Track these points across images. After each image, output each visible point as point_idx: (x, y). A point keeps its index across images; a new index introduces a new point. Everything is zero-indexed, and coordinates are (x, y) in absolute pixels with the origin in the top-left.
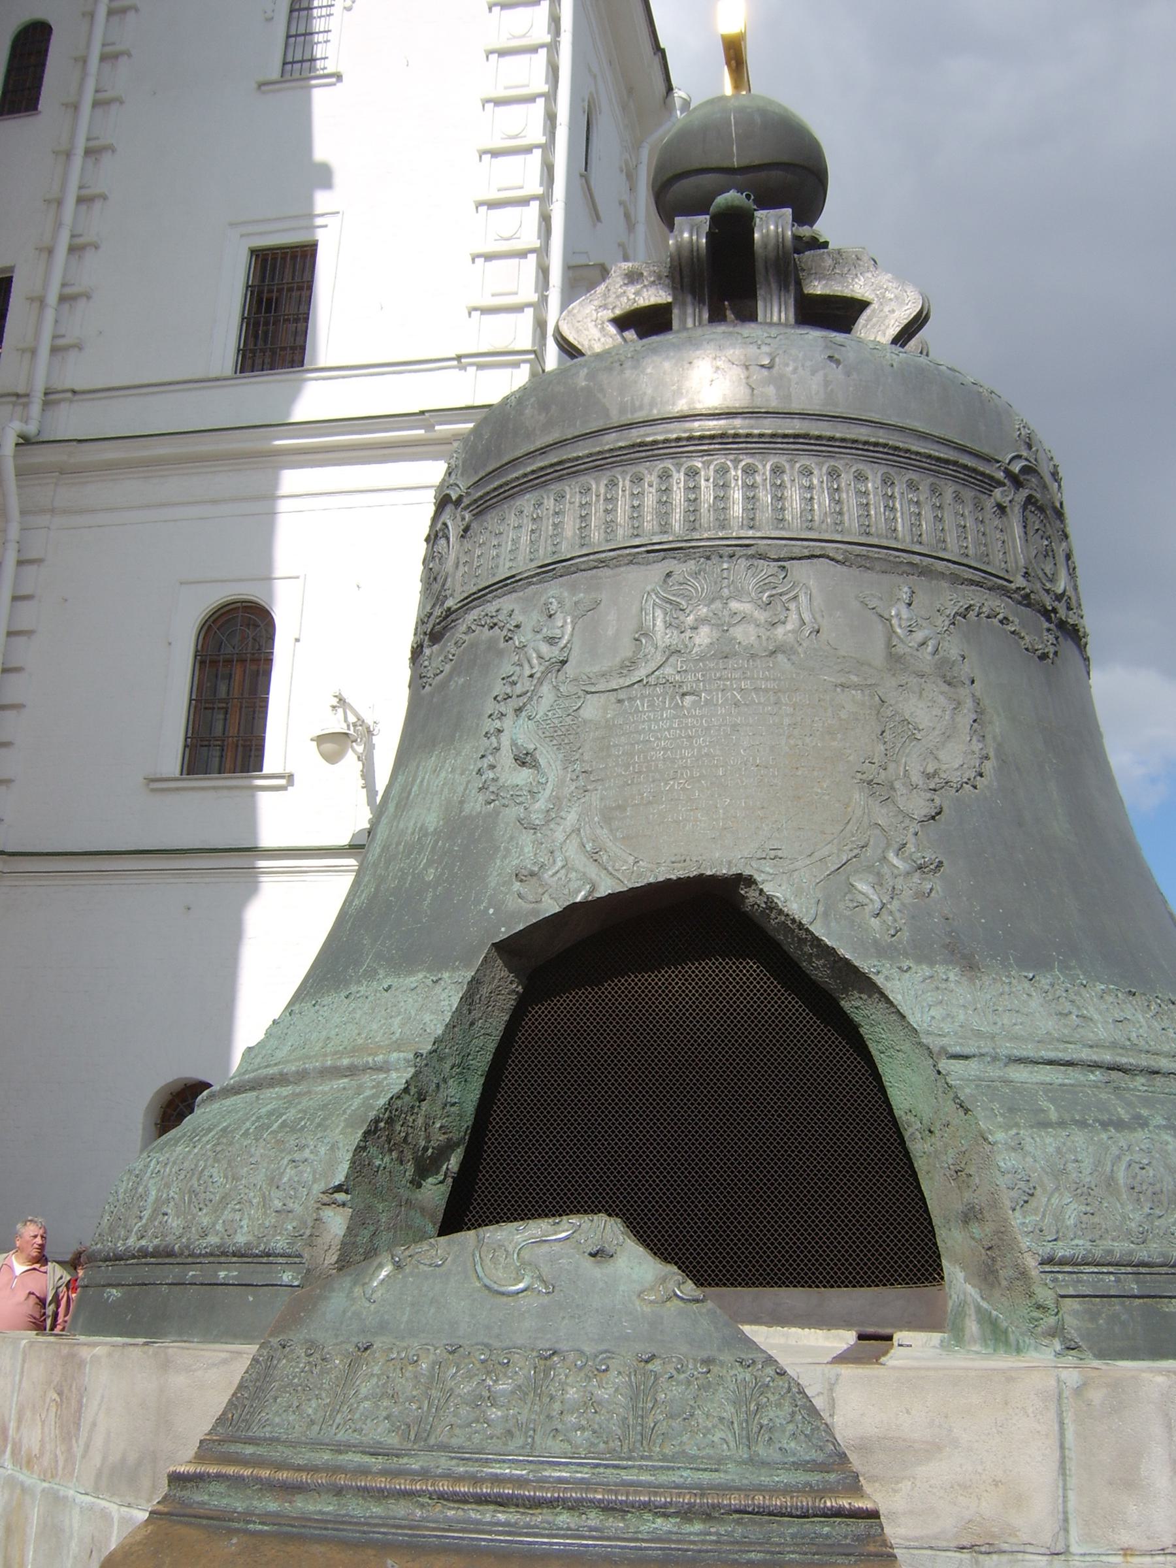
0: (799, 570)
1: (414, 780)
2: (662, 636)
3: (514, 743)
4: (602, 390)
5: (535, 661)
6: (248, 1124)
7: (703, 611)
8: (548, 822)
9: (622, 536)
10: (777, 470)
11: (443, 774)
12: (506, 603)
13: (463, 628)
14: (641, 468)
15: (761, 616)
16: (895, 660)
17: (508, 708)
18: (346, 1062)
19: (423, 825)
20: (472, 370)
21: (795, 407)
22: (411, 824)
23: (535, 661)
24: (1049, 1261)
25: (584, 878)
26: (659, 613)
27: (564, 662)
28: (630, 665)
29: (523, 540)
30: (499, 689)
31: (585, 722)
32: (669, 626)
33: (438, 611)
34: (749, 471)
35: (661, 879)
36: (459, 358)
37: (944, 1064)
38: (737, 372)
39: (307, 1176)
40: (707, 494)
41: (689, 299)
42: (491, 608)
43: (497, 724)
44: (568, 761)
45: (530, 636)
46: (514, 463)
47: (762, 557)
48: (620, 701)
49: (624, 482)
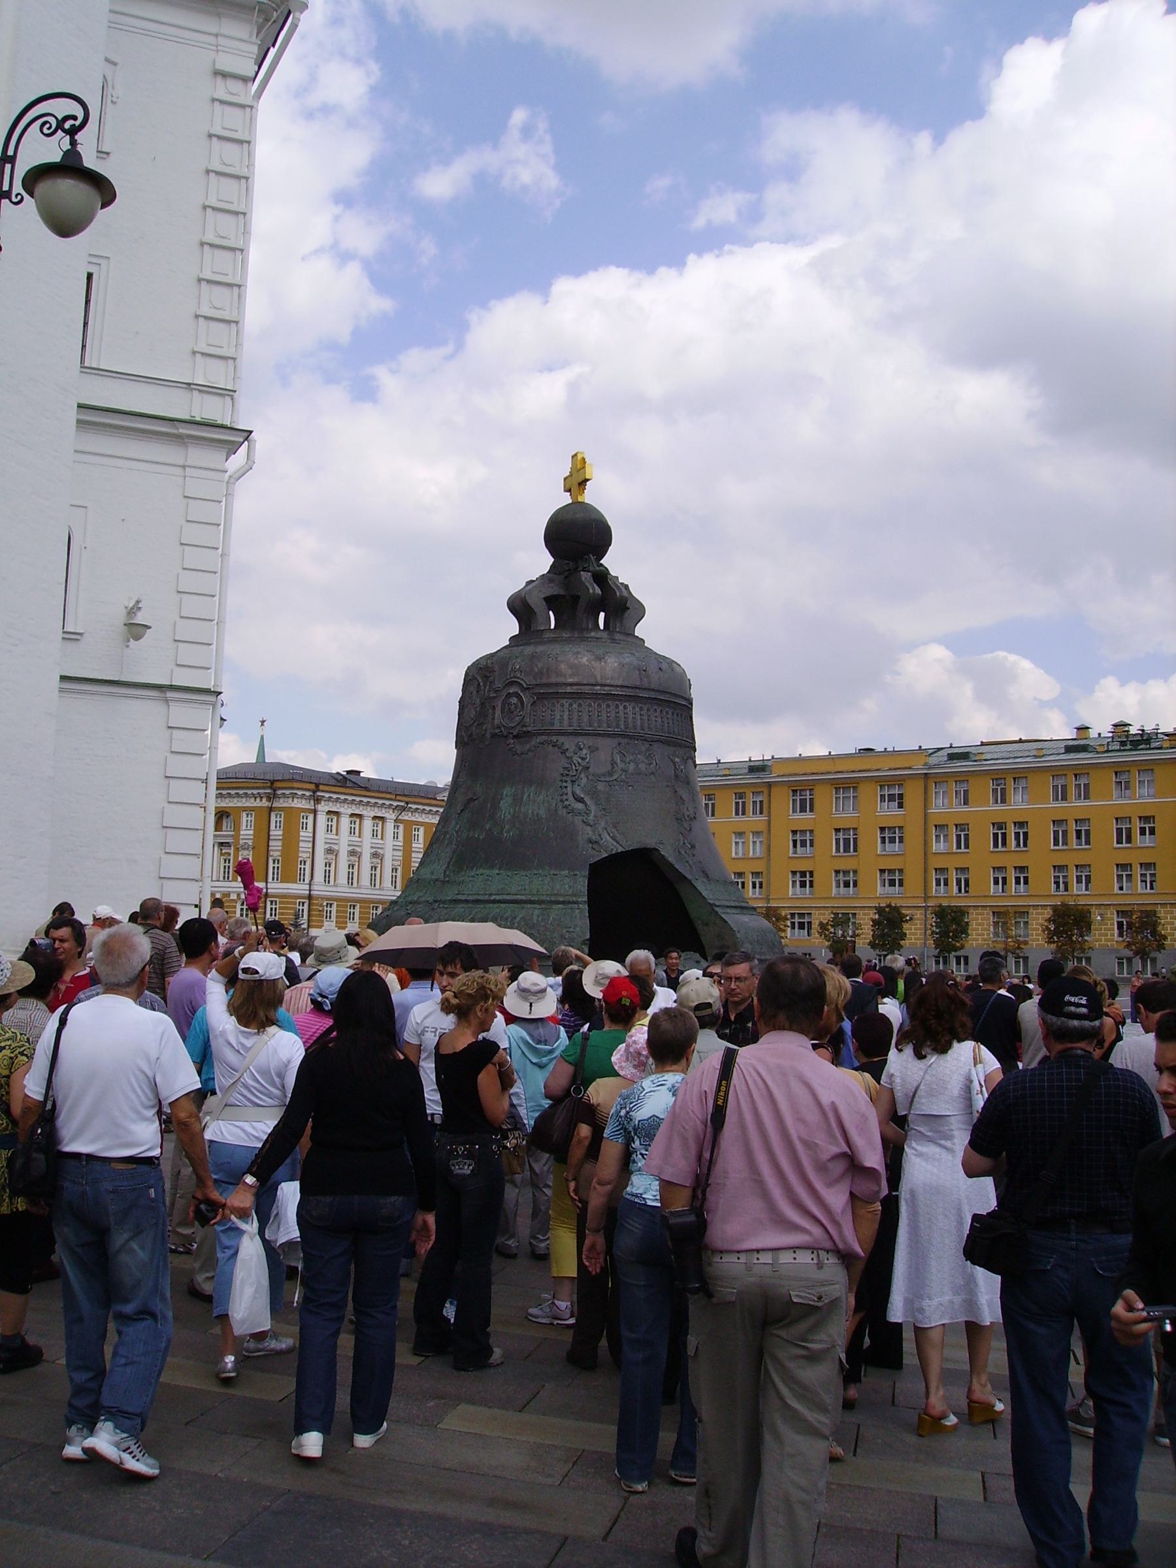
0: (656, 746)
1: (523, 794)
2: (621, 765)
3: (573, 794)
4: (593, 668)
6: (535, 917)
7: (631, 757)
8: (595, 824)
9: (604, 727)
10: (648, 710)
11: (541, 797)
12: (562, 739)
13: (538, 741)
14: (610, 702)
15: (646, 761)
16: (676, 776)
17: (568, 779)
18: (561, 900)
19: (538, 814)
20: (195, 393)
21: (653, 687)
22: (530, 812)
25: (612, 845)
26: (618, 757)
28: (610, 774)
29: (565, 717)
30: (562, 771)
31: (600, 791)
32: (621, 761)
33: (519, 728)
34: (641, 709)
36: (189, 384)
37: (717, 909)
38: (637, 672)
39: (575, 936)
40: (631, 716)
42: (554, 739)
43: (565, 784)
44: (597, 804)
45: (573, 754)
46: (557, 685)
47: (645, 740)
49: (604, 706)
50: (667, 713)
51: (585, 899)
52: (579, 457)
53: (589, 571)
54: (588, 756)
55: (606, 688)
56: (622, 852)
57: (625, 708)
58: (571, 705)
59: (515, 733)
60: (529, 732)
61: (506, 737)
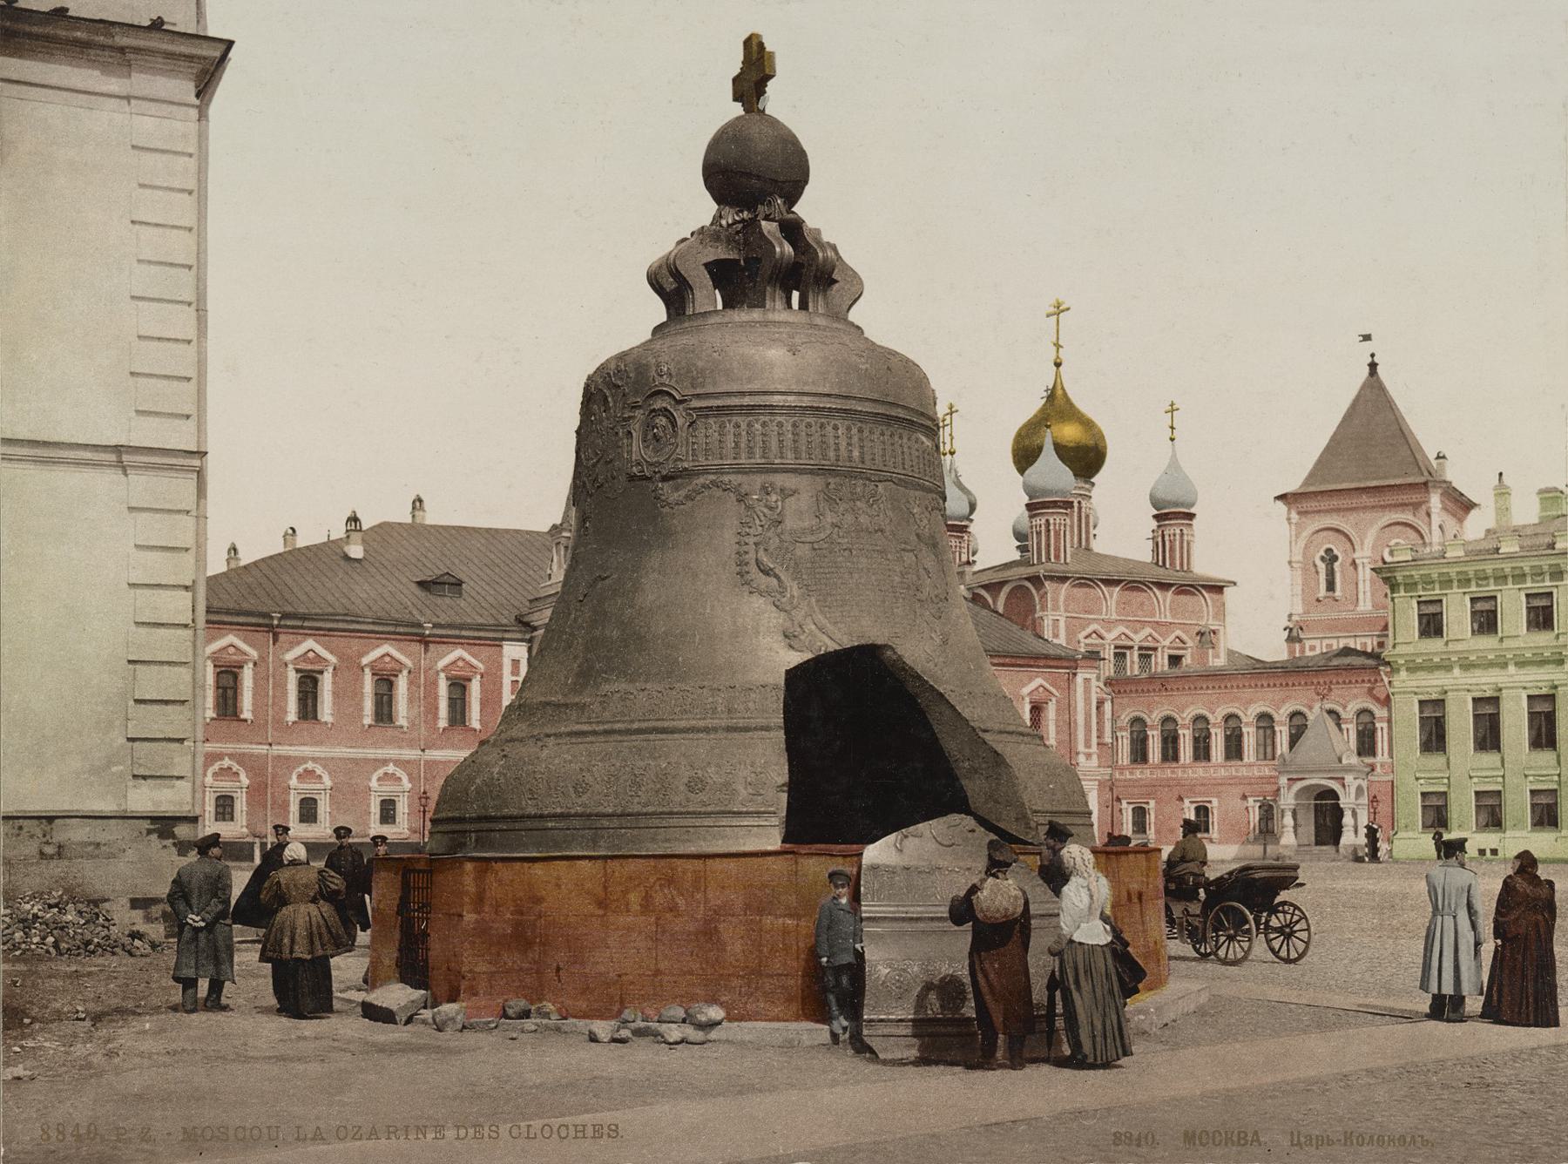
3: (757, 562)
5: (763, 518)
12: (735, 479)
17: (751, 540)
23: (763, 518)
24: (1036, 812)
27: (780, 522)
31: (801, 557)
35: (856, 644)
37: (981, 734)
41: (778, 285)
42: (726, 478)
43: (745, 548)
46: (729, 394)
47: (870, 480)
48: (815, 549)
50: (901, 438)
51: (779, 719)
52: (754, 42)
53: (773, 220)
54: (780, 503)
55: (805, 398)
56: (835, 651)
57: (836, 428)
58: (750, 425)
59: (664, 473)
60: (686, 469)
61: (650, 478)
